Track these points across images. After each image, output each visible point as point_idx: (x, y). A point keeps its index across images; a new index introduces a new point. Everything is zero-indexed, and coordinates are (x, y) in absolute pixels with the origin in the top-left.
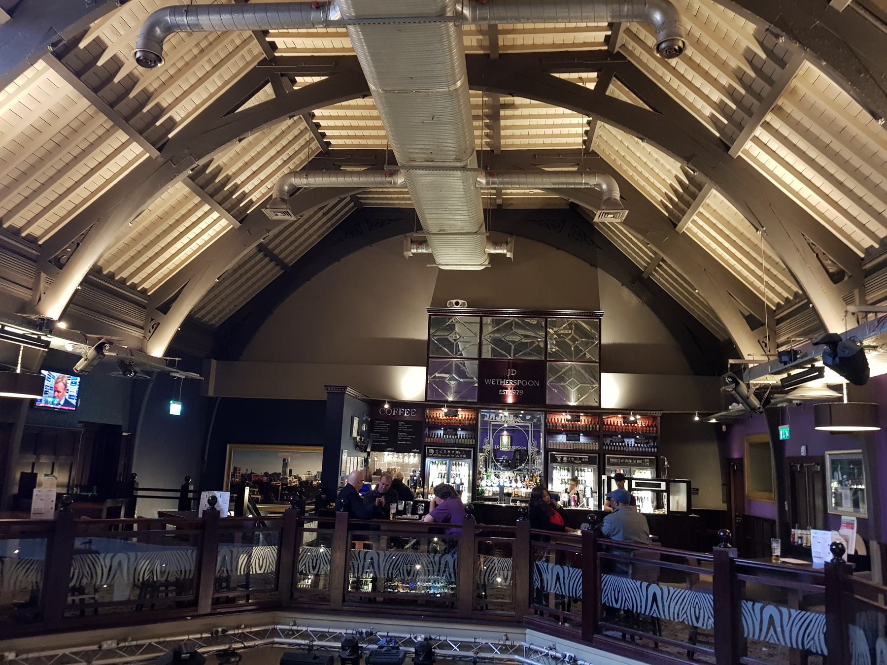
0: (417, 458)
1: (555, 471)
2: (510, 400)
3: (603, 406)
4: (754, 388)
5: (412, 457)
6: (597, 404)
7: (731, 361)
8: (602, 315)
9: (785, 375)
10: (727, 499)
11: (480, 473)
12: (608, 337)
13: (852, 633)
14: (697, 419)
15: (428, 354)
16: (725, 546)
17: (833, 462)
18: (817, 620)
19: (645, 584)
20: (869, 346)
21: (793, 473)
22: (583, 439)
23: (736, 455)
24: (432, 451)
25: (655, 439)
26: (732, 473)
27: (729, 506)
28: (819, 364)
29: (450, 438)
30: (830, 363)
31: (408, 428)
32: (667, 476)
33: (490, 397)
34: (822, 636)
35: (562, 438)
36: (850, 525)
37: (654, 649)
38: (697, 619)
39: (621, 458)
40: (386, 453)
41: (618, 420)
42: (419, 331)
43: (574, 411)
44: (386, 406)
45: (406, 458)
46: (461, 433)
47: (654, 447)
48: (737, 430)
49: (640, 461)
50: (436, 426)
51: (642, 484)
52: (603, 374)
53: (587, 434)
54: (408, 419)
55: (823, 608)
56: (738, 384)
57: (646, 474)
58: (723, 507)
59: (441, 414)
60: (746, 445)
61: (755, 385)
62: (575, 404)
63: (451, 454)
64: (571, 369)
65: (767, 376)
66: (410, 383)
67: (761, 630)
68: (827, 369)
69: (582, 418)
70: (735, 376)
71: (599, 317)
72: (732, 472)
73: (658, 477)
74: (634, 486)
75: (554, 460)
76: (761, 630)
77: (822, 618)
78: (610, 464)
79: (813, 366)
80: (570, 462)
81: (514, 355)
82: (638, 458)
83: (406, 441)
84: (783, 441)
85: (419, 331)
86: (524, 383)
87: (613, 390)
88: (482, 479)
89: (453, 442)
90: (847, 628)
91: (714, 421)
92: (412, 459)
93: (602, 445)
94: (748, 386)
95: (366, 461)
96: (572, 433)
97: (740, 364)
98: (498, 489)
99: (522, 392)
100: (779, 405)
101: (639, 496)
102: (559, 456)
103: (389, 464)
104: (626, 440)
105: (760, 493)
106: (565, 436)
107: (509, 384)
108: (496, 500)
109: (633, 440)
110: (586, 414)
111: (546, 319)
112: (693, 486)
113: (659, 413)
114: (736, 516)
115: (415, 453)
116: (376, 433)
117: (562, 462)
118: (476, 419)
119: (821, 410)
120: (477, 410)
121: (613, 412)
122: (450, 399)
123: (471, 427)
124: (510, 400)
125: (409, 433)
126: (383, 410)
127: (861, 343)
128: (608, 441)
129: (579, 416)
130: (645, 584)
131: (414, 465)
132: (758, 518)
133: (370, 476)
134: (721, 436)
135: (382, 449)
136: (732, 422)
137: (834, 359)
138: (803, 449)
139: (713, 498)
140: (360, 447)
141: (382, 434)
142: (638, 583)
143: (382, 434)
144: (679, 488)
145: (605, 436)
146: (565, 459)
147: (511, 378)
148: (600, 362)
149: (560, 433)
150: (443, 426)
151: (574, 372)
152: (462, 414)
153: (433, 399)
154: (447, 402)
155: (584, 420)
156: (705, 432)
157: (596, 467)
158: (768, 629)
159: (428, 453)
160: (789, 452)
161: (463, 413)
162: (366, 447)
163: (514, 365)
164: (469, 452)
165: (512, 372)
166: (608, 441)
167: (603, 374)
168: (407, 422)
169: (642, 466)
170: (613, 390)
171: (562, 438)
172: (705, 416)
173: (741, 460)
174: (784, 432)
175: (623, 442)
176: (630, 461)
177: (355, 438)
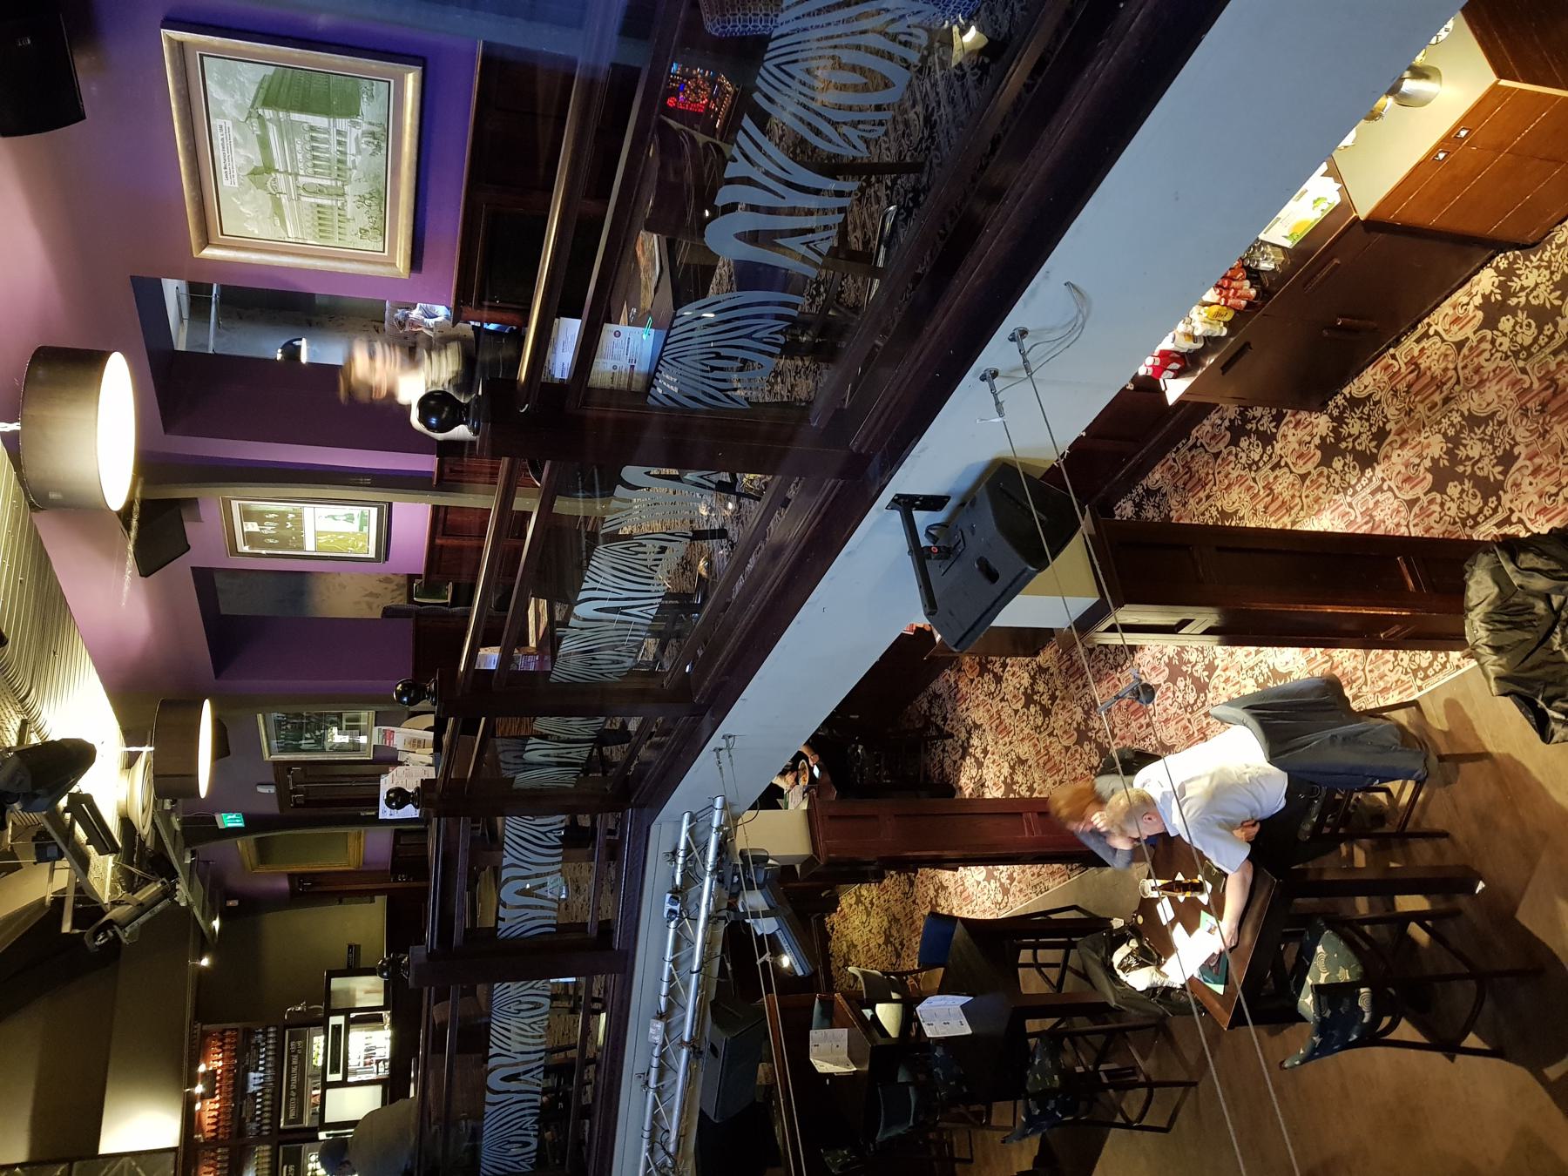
4: (121, 893)
7: (66, 928)
9: (91, 848)
10: (369, 895)
13: (527, 785)
14: (205, 962)
16: (407, 967)
17: (283, 750)
18: (512, 827)
19: (489, 1097)
20: (22, 733)
21: (308, 803)
23: (284, 884)
25: (249, 1033)
26: (318, 889)
27: (380, 892)
28: (63, 803)
30: (47, 801)
32: (320, 1009)
34: (538, 821)
36: (388, 736)
37: (598, 1067)
38: (537, 1006)
41: (208, 1110)
47: (265, 1033)
48: (234, 881)
51: (336, 1057)
55: (499, 820)
56: (110, 923)
58: (381, 901)
60: (263, 869)
61: (114, 890)
65: (93, 876)
67: (542, 907)
68: (74, 790)
70: (93, 928)
72: (315, 890)
74: (338, 1077)
76: (542, 907)
77: (512, 822)
78: (300, 1119)
79: (66, 810)
82: (287, 1060)
84: (247, 818)
90: (518, 790)
91: (216, 924)
94: (115, 904)
97: (75, 911)
100: (177, 827)
101: (363, 1054)
104: (252, 1089)
105: (351, 850)
109: (252, 1075)
112: (343, 966)
114: (396, 880)
119: (171, 782)
127: (9, 750)
130: (489, 1097)
132: (395, 852)
134: (245, 909)
136: (217, 892)
137: (36, 796)
138: (261, 789)
139: (366, 922)
142: (488, 1109)
144: (341, 991)
156: (240, 945)
158: (537, 896)
160: (273, 808)
169: (303, 1054)
172: (205, 943)
173: (291, 876)
174: (230, 820)
176: (294, 1079)
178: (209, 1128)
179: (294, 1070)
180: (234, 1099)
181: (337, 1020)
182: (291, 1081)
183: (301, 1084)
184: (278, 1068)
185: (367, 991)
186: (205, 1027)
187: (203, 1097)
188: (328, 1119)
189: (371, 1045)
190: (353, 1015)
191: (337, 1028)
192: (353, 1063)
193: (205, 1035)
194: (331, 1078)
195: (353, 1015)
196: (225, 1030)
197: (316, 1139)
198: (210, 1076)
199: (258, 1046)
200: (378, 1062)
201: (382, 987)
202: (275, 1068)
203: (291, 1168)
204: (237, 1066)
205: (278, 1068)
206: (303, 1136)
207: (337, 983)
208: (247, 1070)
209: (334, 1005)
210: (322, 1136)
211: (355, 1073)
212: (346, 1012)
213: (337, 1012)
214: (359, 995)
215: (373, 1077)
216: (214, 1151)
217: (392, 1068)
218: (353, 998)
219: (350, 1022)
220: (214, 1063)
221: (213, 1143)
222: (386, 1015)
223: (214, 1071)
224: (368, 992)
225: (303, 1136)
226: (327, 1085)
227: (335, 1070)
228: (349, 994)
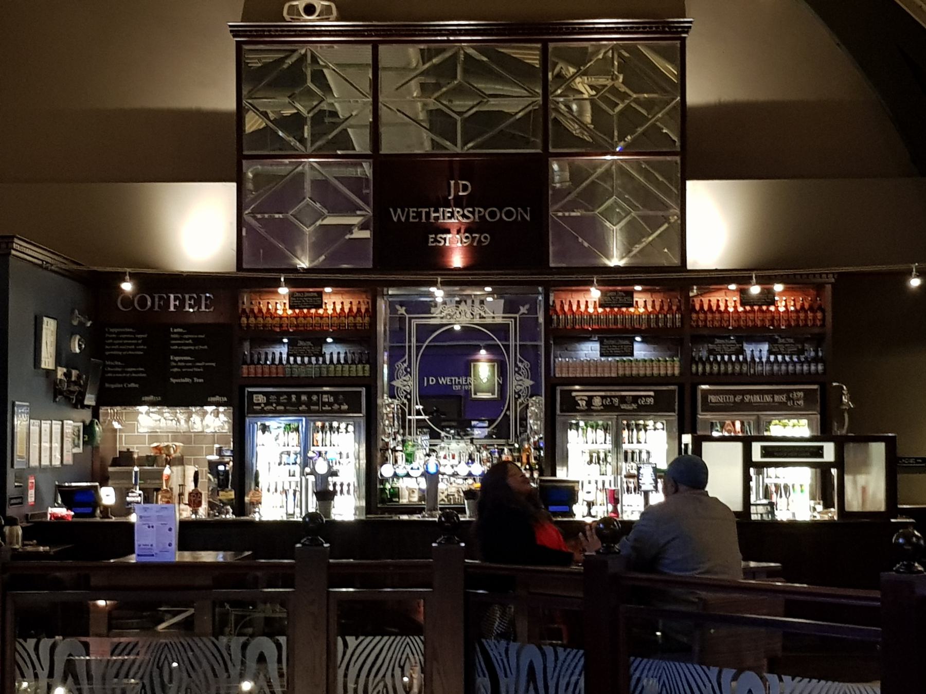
0: (223, 417)
1: (572, 434)
2: (457, 261)
3: (690, 266)
5: (209, 419)
6: (676, 261)
8: (687, 30)
11: (386, 447)
12: (697, 94)
15: (240, 148)
22: (641, 351)
24: (261, 399)
29: (306, 364)
31: (196, 342)
33: (405, 254)
35: (590, 351)
39: (735, 393)
40: (143, 409)
41: (727, 299)
42: (216, 91)
43: (618, 283)
44: (127, 287)
45: (196, 418)
46: (333, 350)
47: (816, 360)
49: (783, 398)
50: (269, 333)
52: (689, 184)
53: (653, 334)
54: (195, 320)
57: (797, 428)
59: (280, 302)
62: (622, 263)
63: (309, 403)
64: (608, 174)
66: (199, 227)
69: (639, 299)
71: (678, 34)
73: (825, 433)
75: (571, 406)
78: (708, 408)
80: (608, 408)
81: (462, 149)
83: (191, 375)
85: (216, 91)
86: (493, 215)
87: (715, 223)
88: (385, 461)
89: (313, 373)
92: (213, 421)
93: (688, 361)
95: (88, 430)
96: (616, 337)
98: (423, 484)
99: (486, 239)
101: (781, 482)
102: (579, 393)
103: (154, 436)
104: (748, 348)
106: (597, 346)
107: (454, 218)
108: (419, 510)
110: (651, 285)
111: (545, 44)
113: (828, 275)
115: (218, 404)
116: (113, 358)
117: (589, 410)
118: (372, 313)
120: (372, 290)
121: (713, 279)
122: (303, 263)
123: (358, 334)
124: (457, 261)
125: (198, 356)
126: (127, 300)
128: (704, 354)
129: (631, 294)
131: (216, 437)
133: (104, 469)
135: (131, 399)
140: (62, 395)
141: (128, 361)
143: (128, 361)
145: (698, 339)
146: (597, 402)
147: (459, 202)
148: (683, 153)
149: (585, 337)
150: (285, 333)
151: (617, 182)
152: (334, 302)
153: (256, 265)
154: (295, 270)
155: (643, 302)
157: (674, 416)
159: (251, 403)
161: (338, 299)
162: (82, 395)
163: (465, 168)
164: (349, 397)
165: (460, 188)
166: (704, 354)
167: (689, 184)
168: (191, 328)
169: (787, 409)
170: (715, 223)
171: (590, 351)
175: (741, 351)
177: (48, 372)
178: (705, 300)
179: (768, 398)
180: (738, 328)
181: (829, 452)
182: (757, 395)
183: (751, 407)
184: (772, 378)
185: (867, 488)
186: (829, 287)
187: (743, 292)
188: (706, 446)
189: (795, 498)
190: (834, 471)
191: (819, 452)
192: (772, 471)
193: (819, 288)
194: (756, 447)
195: (834, 471)
196: (823, 311)
197: (681, 431)
198: (768, 298)
199: (800, 352)
200: (772, 505)
201: (869, 508)
202: (772, 373)
203: (651, 401)
204: (777, 329)
205: (772, 378)
206: (687, 410)
207: (878, 450)
208: (772, 341)
209: (850, 448)
210: (687, 439)
211: (758, 473)
212: (839, 463)
213: (839, 453)
214: (862, 479)
215: (753, 499)
216: (679, 309)
217: (761, 524)
218: (856, 471)
219: (823, 470)
220: (784, 301)
221: (688, 308)
222: (833, 514)
223: (773, 302)
224: (864, 490)
225: (687, 410)
226: (747, 442)
227: (766, 452)
228: (863, 465)
